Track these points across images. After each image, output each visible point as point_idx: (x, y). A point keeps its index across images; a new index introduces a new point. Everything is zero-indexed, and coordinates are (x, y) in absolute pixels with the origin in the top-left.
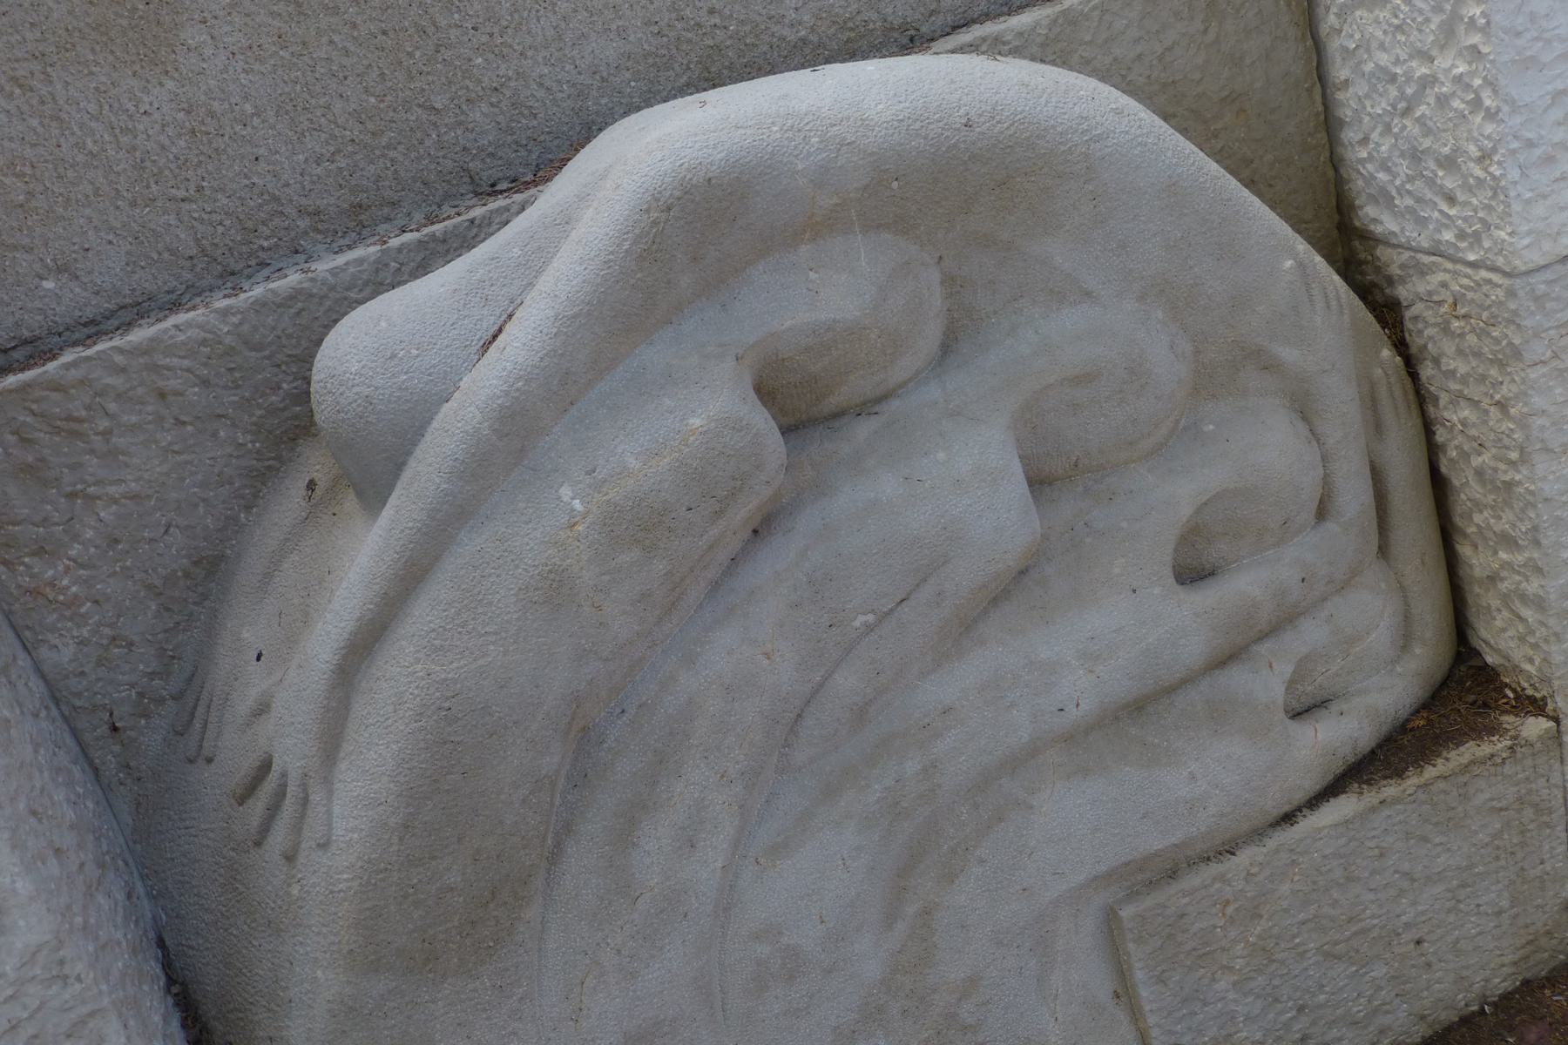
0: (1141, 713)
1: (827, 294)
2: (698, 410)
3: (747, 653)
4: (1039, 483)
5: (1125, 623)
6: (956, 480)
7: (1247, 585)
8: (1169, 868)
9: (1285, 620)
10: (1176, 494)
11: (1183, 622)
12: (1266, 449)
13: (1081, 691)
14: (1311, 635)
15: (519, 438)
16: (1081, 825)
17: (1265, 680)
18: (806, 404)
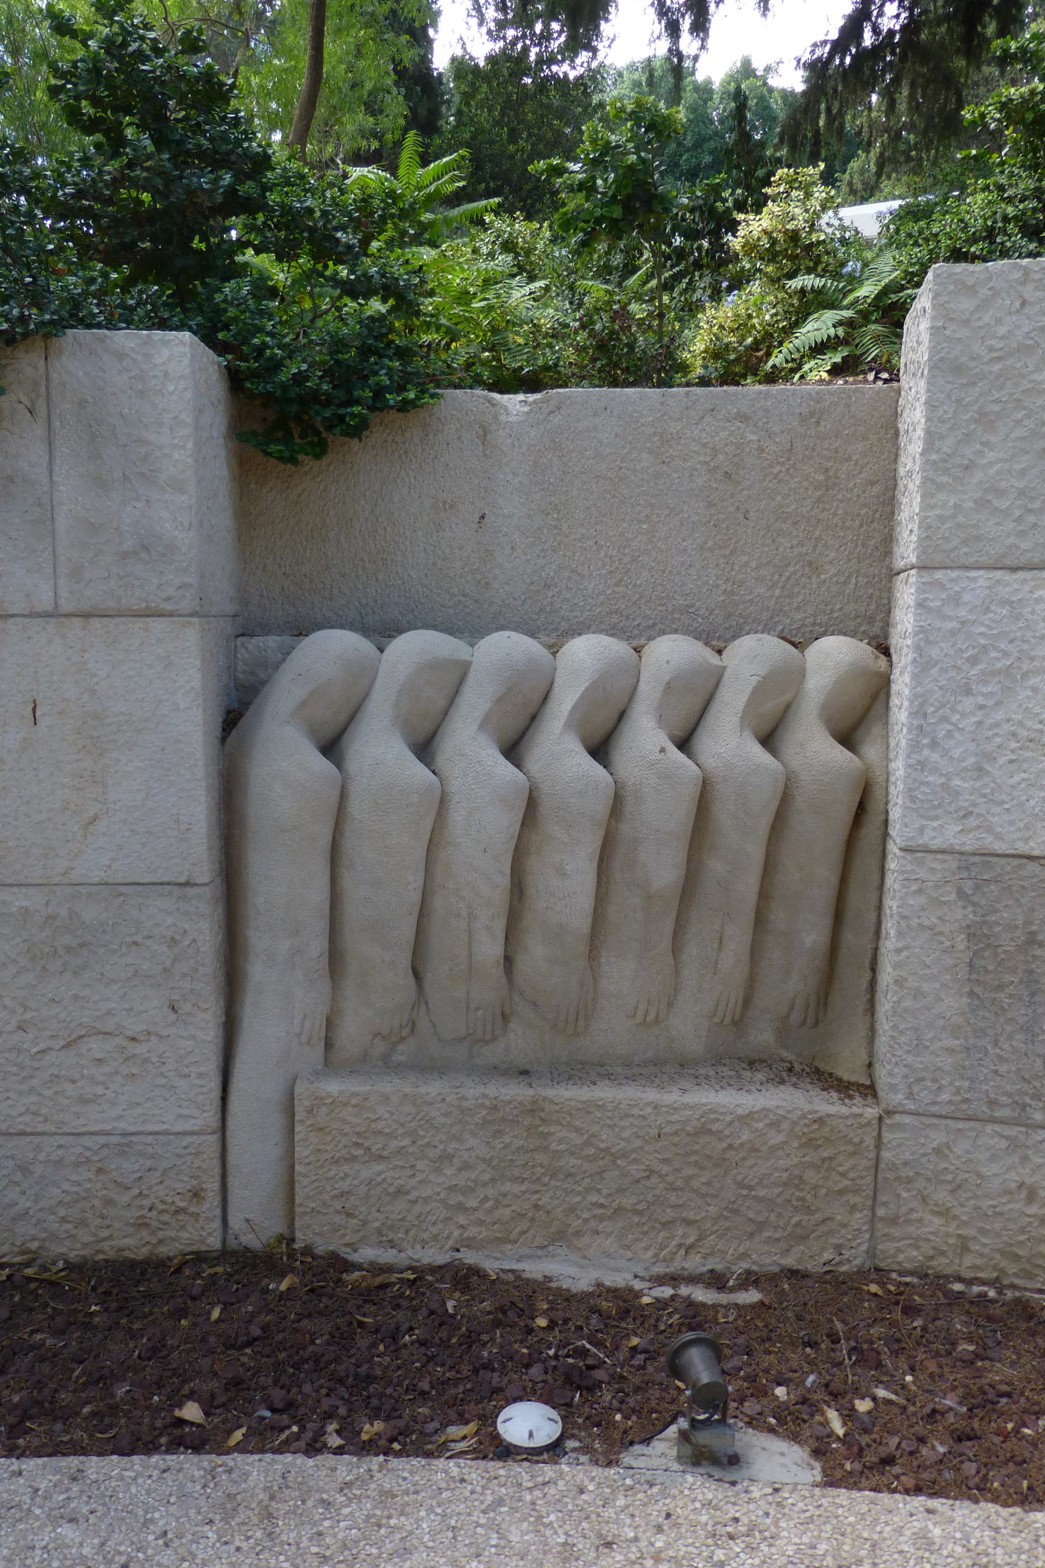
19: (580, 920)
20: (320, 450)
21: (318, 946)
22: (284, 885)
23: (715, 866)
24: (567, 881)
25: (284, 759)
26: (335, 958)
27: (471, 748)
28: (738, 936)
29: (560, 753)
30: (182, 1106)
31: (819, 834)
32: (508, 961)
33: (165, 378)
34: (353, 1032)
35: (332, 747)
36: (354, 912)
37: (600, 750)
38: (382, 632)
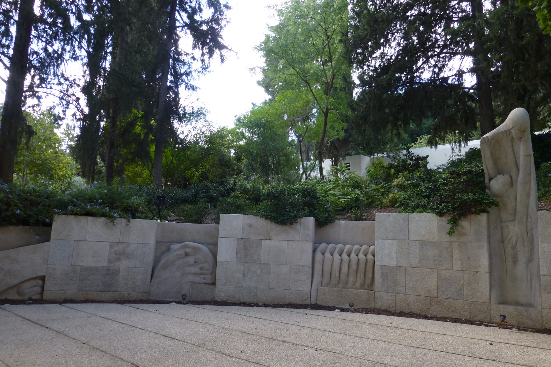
0: (196, 274)
1: (189, 250)
2: (182, 252)
3: (179, 262)
4: (195, 262)
5: (195, 269)
6: (191, 260)
7: (203, 271)
8: (195, 283)
9: (204, 274)
10: (201, 265)
11: (199, 271)
12: (206, 266)
13: (193, 271)
14: (206, 276)
15: (175, 250)
16: (190, 278)
17: (203, 276)
18: (186, 254)
19: (346, 272)
20: (323, 226)
21: (321, 273)
22: (318, 267)
23: (360, 268)
24: (345, 269)
25: (319, 255)
26: (323, 276)
27: (336, 255)
28: (362, 275)
29: (345, 256)
30: (307, 288)
31: (370, 265)
32: (339, 276)
33: (311, 221)
34: (324, 283)
35: (323, 254)
36: (325, 270)
37: (349, 256)
38: (328, 244)
